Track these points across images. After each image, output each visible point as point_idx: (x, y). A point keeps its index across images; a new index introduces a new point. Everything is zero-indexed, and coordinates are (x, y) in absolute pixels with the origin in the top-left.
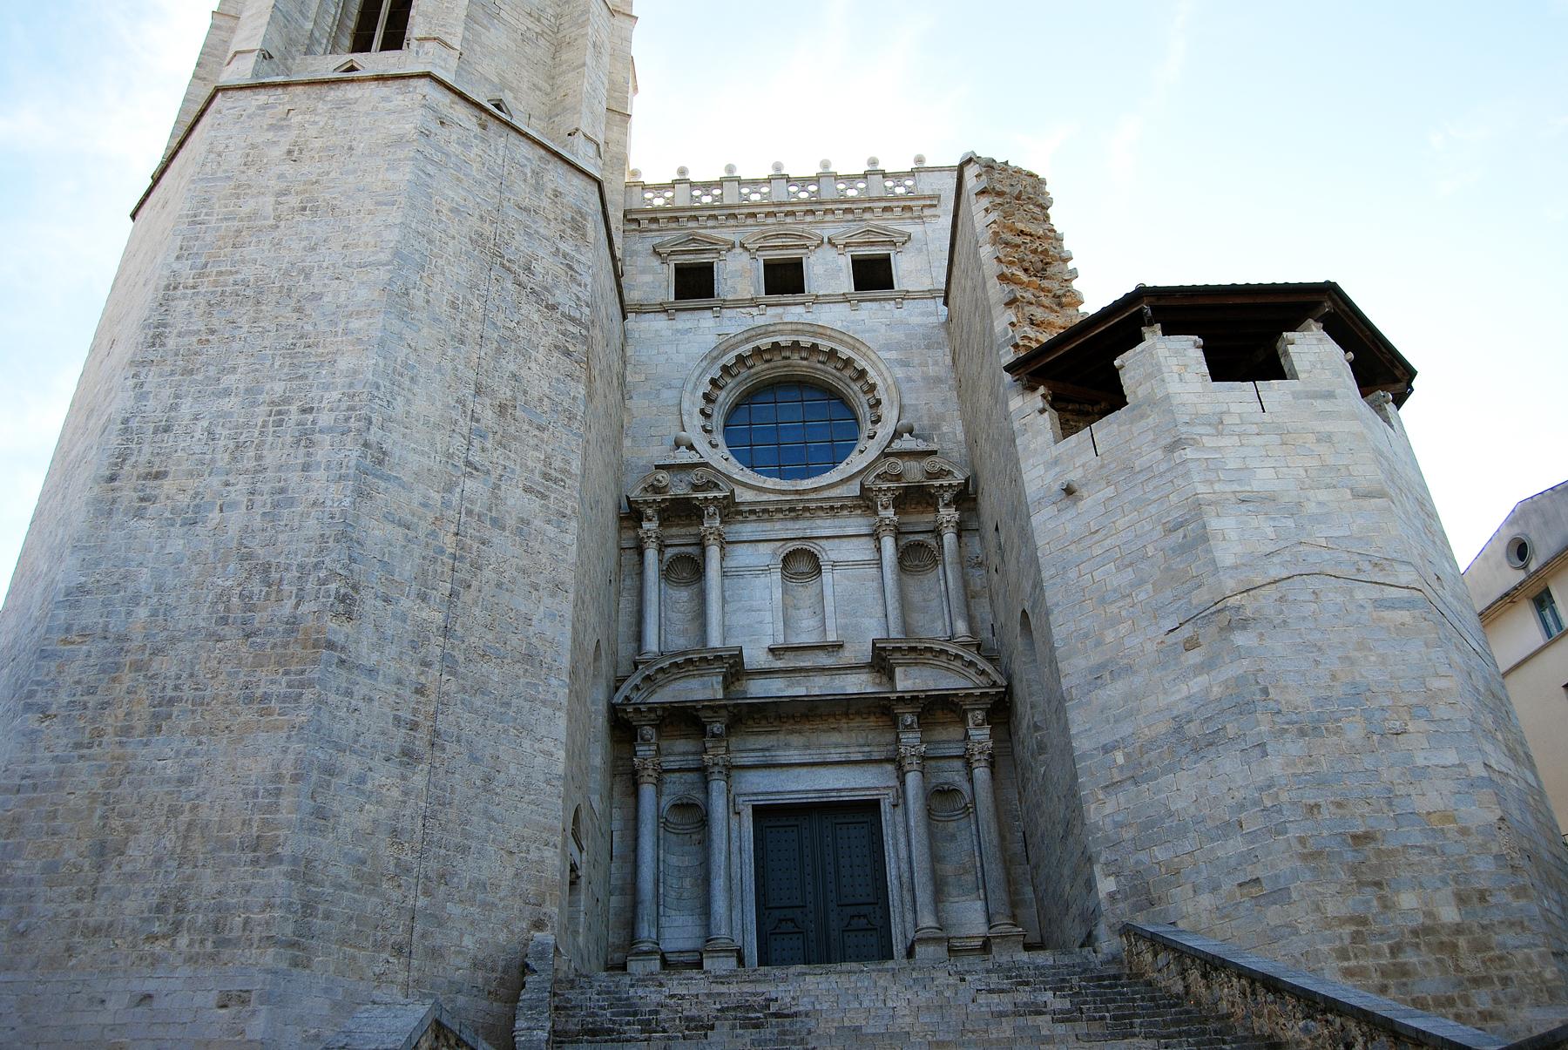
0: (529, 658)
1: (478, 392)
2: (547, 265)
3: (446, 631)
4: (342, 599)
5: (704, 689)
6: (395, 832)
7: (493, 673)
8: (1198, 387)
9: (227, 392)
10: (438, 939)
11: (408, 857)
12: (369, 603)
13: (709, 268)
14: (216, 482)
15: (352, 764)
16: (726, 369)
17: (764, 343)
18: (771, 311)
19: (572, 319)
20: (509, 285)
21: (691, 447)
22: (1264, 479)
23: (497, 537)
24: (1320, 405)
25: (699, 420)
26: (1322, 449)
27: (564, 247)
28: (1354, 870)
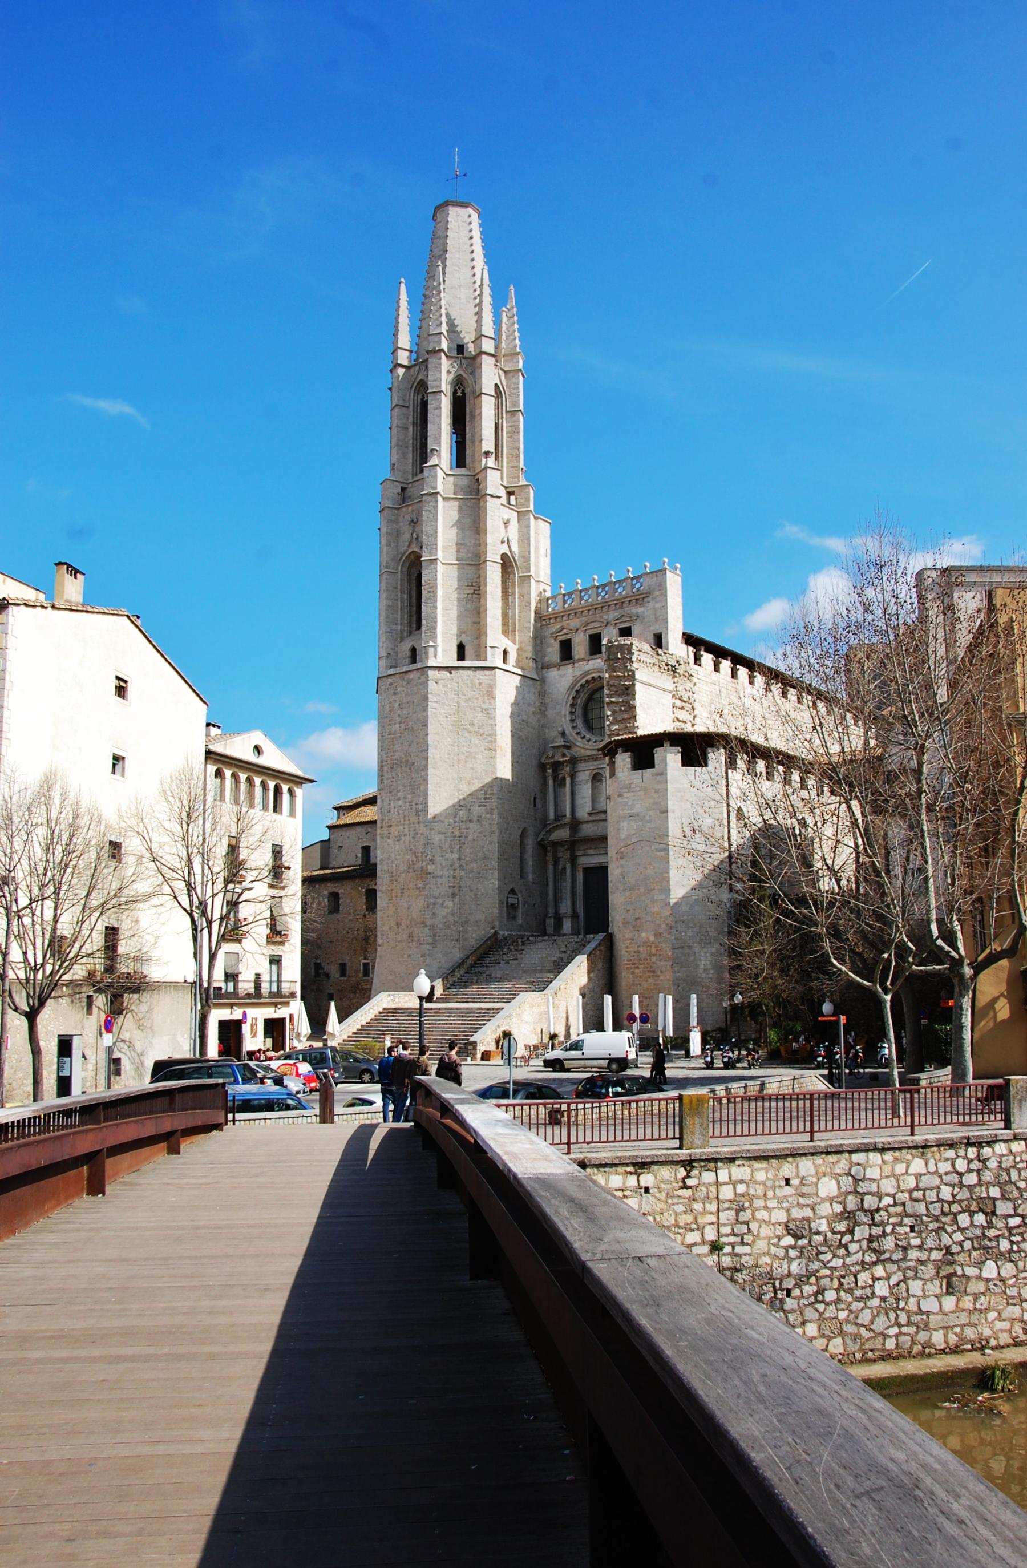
0: (485, 858)
1: (460, 779)
2: (480, 716)
3: (459, 859)
4: (431, 860)
5: (563, 834)
6: (453, 915)
7: (474, 866)
8: (626, 774)
9: (399, 799)
10: (466, 936)
11: (456, 919)
12: (438, 859)
13: (570, 641)
14: (401, 828)
15: (440, 901)
16: (577, 691)
17: (589, 677)
18: (591, 662)
19: (490, 735)
20: (467, 735)
21: (563, 734)
22: (638, 808)
23: (471, 825)
24: (658, 778)
25: (568, 718)
26: (656, 795)
27: (484, 706)
28: (634, 927)
